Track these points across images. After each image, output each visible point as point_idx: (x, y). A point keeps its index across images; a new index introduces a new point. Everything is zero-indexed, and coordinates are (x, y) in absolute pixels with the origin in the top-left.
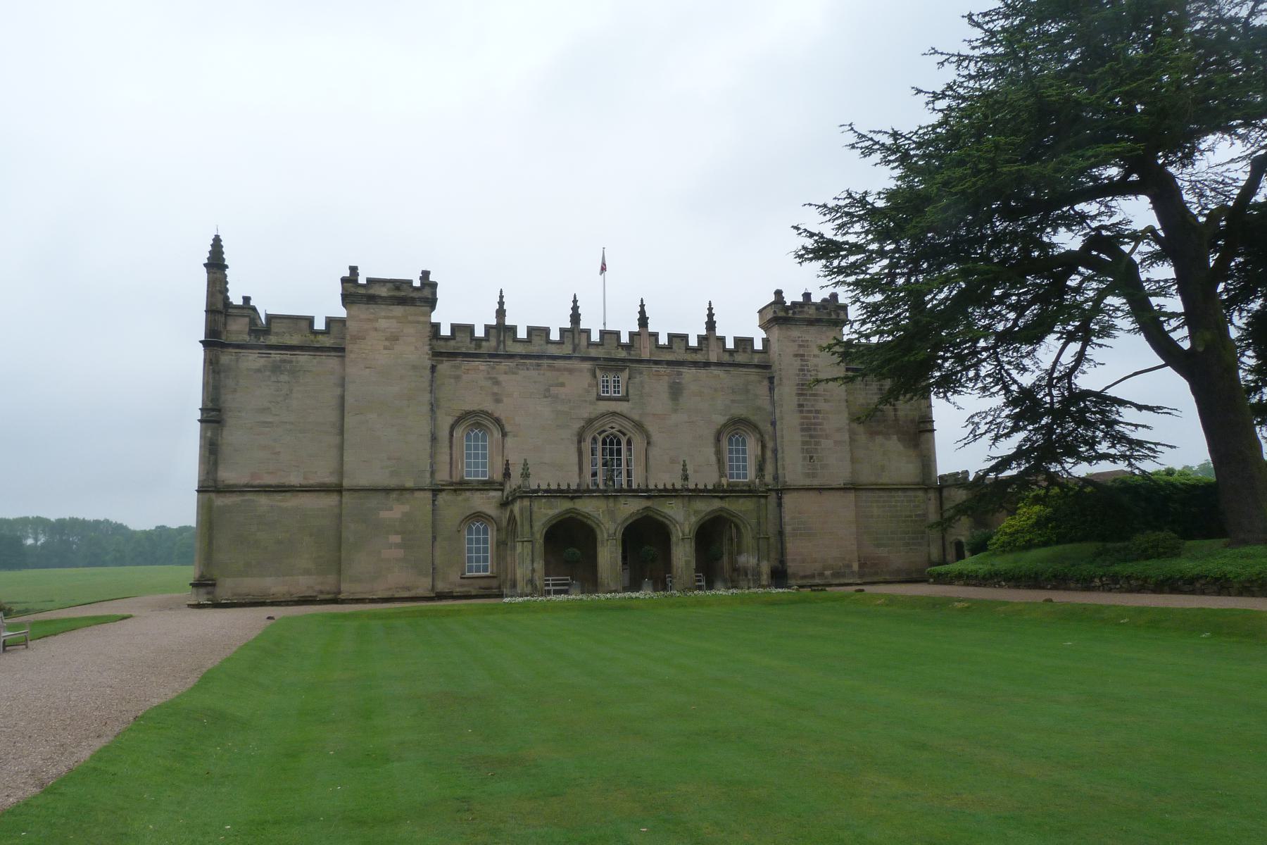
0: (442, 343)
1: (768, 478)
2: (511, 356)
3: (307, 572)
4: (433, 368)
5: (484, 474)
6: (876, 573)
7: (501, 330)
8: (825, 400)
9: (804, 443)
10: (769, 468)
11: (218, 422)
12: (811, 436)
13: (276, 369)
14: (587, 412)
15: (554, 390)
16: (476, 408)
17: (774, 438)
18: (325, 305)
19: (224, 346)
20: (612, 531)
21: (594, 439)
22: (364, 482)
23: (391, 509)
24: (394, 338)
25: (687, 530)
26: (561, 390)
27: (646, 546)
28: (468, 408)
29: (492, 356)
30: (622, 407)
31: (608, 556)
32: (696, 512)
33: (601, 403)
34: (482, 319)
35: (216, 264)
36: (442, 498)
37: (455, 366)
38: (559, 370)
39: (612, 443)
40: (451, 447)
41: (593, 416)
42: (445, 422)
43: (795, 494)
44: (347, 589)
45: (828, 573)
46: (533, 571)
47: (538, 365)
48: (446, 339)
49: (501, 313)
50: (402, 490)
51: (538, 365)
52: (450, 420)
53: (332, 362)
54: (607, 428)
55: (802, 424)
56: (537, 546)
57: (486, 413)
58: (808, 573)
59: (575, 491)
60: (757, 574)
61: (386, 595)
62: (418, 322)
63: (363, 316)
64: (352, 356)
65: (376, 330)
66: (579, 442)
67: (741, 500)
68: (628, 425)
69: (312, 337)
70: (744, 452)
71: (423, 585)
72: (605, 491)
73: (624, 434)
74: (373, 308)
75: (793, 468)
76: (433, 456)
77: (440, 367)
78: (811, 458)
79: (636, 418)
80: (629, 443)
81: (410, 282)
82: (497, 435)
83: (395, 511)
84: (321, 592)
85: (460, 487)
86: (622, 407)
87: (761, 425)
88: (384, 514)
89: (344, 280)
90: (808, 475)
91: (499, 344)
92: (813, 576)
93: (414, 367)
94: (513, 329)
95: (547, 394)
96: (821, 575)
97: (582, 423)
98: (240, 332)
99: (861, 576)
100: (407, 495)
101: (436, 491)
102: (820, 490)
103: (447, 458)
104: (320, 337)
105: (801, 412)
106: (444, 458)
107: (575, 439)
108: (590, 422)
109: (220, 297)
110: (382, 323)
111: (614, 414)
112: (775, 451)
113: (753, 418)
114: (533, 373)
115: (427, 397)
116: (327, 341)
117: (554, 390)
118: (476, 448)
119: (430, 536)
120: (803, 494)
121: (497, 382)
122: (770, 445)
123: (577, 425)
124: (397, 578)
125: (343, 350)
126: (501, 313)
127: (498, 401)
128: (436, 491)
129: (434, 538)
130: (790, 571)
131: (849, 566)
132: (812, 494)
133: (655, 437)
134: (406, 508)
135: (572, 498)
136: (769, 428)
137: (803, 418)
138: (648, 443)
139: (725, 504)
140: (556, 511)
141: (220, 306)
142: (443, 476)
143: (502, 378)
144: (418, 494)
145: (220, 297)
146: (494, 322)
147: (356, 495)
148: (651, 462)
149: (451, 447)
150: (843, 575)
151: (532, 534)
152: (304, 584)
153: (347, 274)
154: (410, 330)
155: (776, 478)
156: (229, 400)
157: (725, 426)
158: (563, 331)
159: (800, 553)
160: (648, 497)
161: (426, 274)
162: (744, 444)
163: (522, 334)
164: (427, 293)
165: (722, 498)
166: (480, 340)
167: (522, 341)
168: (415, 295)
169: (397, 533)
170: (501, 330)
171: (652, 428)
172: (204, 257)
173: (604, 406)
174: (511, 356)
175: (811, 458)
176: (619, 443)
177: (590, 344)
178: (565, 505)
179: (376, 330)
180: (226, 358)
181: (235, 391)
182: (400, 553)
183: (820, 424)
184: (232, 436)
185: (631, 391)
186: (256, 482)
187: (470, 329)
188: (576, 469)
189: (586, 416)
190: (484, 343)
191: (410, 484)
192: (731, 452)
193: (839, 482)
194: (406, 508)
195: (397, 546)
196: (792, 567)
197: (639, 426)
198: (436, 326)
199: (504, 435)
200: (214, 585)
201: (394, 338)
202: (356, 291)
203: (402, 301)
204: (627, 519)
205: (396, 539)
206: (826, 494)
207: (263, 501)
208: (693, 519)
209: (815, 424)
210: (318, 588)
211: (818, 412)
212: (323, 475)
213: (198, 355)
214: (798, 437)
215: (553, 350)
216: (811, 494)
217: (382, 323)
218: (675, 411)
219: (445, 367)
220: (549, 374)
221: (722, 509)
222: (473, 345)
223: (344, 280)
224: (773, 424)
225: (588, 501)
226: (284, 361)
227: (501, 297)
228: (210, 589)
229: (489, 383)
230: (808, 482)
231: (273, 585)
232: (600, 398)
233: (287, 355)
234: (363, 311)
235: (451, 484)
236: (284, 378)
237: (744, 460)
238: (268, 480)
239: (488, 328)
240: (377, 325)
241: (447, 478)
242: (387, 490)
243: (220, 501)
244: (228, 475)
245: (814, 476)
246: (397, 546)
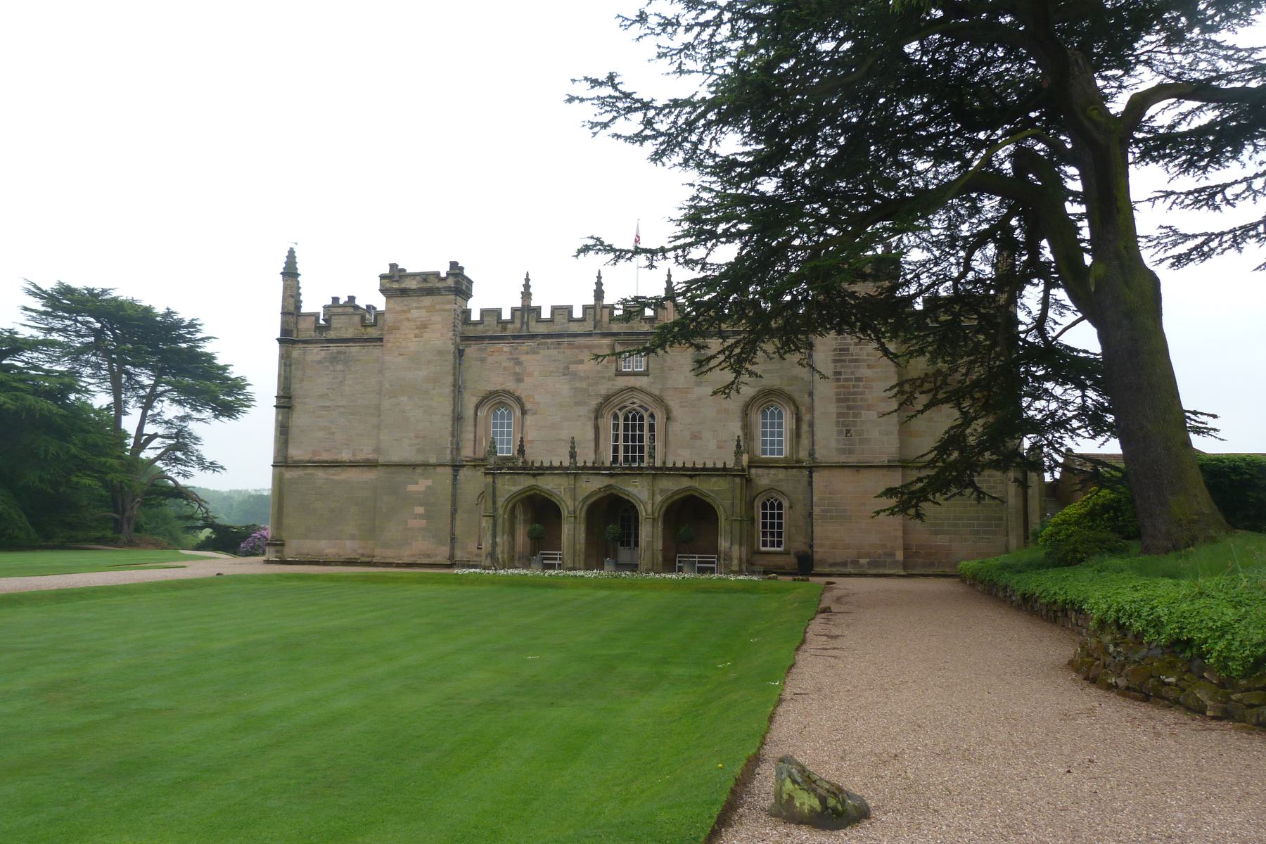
0: (471, 328)
1: (803, 454)
2: (533, 337)
3: (353, 537)
4: (460, 353)
5: (508, 450)
6: (932, 564)
7: (527, 311)
8: (869, 367)
9: (839, 415)
10: (805, 442)
11: (289, 408)
12: (849, 408)
13: (334, 359)
14: (604, 389)
15: (573, 368)
16: (499, 388)
17: (811, 409)
19: (294, 342)
20: (571, 508)
21: (616, 417)
22: (395, 458)
23: (417, 483)
24: (423, 326)
25: (650, 510)
26: (581, 367)
27: (612, 523)
28: (492, 388)
29: (515, 337)
30: (642, 382)
31: (649, 534)
32: (661, 491)
33: (620, 378)
34: (507, 302)
35: (290, 273)
36: (463, 473)
37: (480, 349)
38: (579, 347)
39: (634, 418)
40: (475, 426)
41: (611, 392)
42: (470, 402)
43: (826, 473)
44: (380, 553)
45: (863, 561)
46: (494, 545)
47: (559, 344)
48: (476, 324)
49: (526, 294)
50: (426, 465)
51: (559, 344)
52: (475, 400)
53: (374, 351)
54: (627, 403)
55: (838, 394)
56: (500, 521)
57: (508, 393)
58: (839, 560)
59: (538, 468)
60: (729, 558)
61: (406, 560)
62: (445, 310)
63: (398, 308)
64: (389, 345)
65: (408, 320)
66: (596, 418)
67: (714, 479)
68: (648, 399)
69: (363, 330)
70: (780, 425)
71: (442, 554)
72: (568, 468)
73: (647, 410)
74: (407, 300)
75: (827, 443)
76: (456, 434)
77: (467, 350)
78: (848, 431)
79: (657, 393)
80: (652, 416)
81: (437, 274)
82: (518, 413)
83: (419, 485)
84: (363, 555)
86: (642, 382)
87: (796, 396)
88: (412, 488)
89: (382, 277)
90: (842, 451)
91: (526, 327)
92: (845, 564)
93: (440, 353)
94: (538, 310)
95: (566, 372)
96: (855, 563)
97: (600, 400)
98: (308, 330)
99: (905, 567)
100: (431, 470)
101: (456, 467)
102: (858, 467)
103: (471, 436)
104: (369, 330)
105: (838, 380)
106: (468, 436)
107: (592, 416)
108: (608, 398)
109: (292, 300)
110: (415, 314)
111: (632, 389)
112: (811, 425)
113: (787, 389)
114: (554, 352)
115: (450, 379)
116: (373, 333)
117: (573, 368)
118: (502, 426)
119: (448, 507)
120: (837, 472)
121: (518, 362)
122: (806, 418)
123: (594, 402)
124: (420, 546)
125: (381, 340)
126: (526, 294)
127: (519, 380)
129: (454, 511)
130: (816, 557)
131: (892, 555)
132: (847, 473)
133: (677, 411)
134: (429, 482)
135: (534, 475)
136: (806, 398)
137: (838, 387)
138: (668, 418)
139: (695, 483)
140: (520, 488)
141: (292, 309)
142: (467, 452)
143: (523, 358)
144: (439, 470)
145: (292, 300)
146: (519, 304)
147: (389, 470)
148: (671, 438)
149: (475, 426)
150: (884, 565)
151: (495, 509)
152: (350, 547)
153: (386, 271)
154: (437, 318)
155: (812, 454)
156: (296, 388)
157: (753, 398)
158: (585, 308)
159: (829, 537)
160: (611, 475)
161: (454, 265)
162: (780, 417)
163: (546, 314)
164: (451, 282)
165: (691, 476)
166: (507, 322)
167: (545, 321)
168: (440, 285)
169: (421, 505)
170: (527, 311)
171: (673, 404)
172: (281, 267)
173: (622, 382)
174: (533, 337)
175: (848, 431)
176: (642, 418)
177: (613, 319)
178: (530, 482)
179: (408, 320)
180: (296, 352)
181: (302, 380)
182: (423, 522)
183: (863, 393)
184: (299, 419)
185: (651, 365)
186: (317, 458)
187: (498, 312)
188: (592, 445)
189: (603, 392)
190: (509, 326)
191: (433, 460)
192: (764, 425)
193: (885, 459)
194: (429, 482)
195: (421, 516)
196: (819, 553)
197: (659, 400)
198: (467, 313)
199: (524, 412)
200: (283, 545)
201: (423, 326)
202: (395, 282)
203: (431, 292)
204: (587, 497)
205: (420, 510)
206: (862, 471)
207: (321, 474)
208: (659, 498)
209: (854, 393)
210: (360, 551)
211: (859, 379)
212: (366, 453)
213: (275, 350)
214: (833, 408)
215: (574, 328)
216: (846, 472)
217: (415, 314)
218: (699, 384)
219: (472, 351)
220: (568, 352)
221: (689, 489)
222: (499, 329)
223: (382, 277)
224: (811, 394)
225: (550, 478)
226: (339, 353)
227: (527, 280)
228: (279, 548)
229: (511, 364)
230: (842, 459)
231: (326, 547)
232: (619, 373)
233: (342, 347)
234: (399, 304)
235: (475, 460)
236: (339, 367)
237: (780, 434)
238: (326, 456)
239: (514, 310)
240: (409, 315)
241: (471, 454)
242: (414, 466)
243: (289, 474)
244: (295, 453)
245: (851, 452)
246: (421, 516)
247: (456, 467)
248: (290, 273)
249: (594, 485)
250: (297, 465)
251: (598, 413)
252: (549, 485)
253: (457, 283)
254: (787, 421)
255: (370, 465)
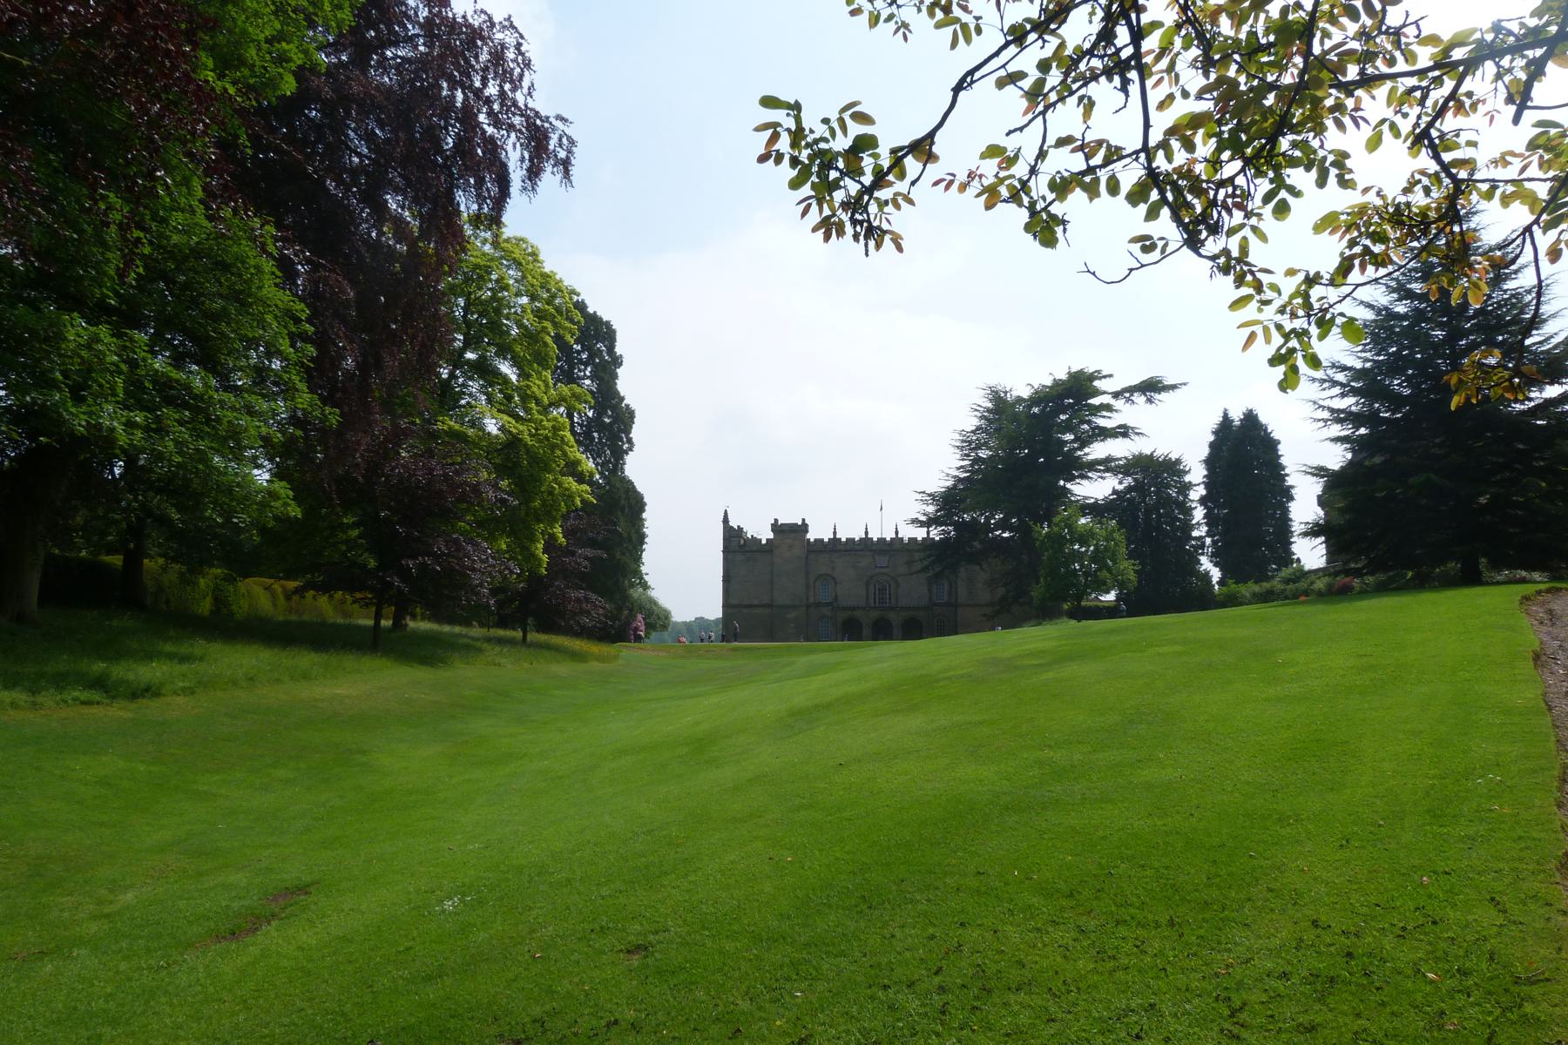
18: (766, 534)
34: (827, 536)
85: (818, 605)
91: (835, 547)
128: (808, 606)
142: (811, 600)
202: (776, 527)
244: (734, 601)
247: (808, 606)
248: (726, 520)
249: (875, 614)
250: (733, 606)
251: (867, 584)
252: (858, 613)
253: (804, 528)
254: (946, 586)
255: (770, 606)
